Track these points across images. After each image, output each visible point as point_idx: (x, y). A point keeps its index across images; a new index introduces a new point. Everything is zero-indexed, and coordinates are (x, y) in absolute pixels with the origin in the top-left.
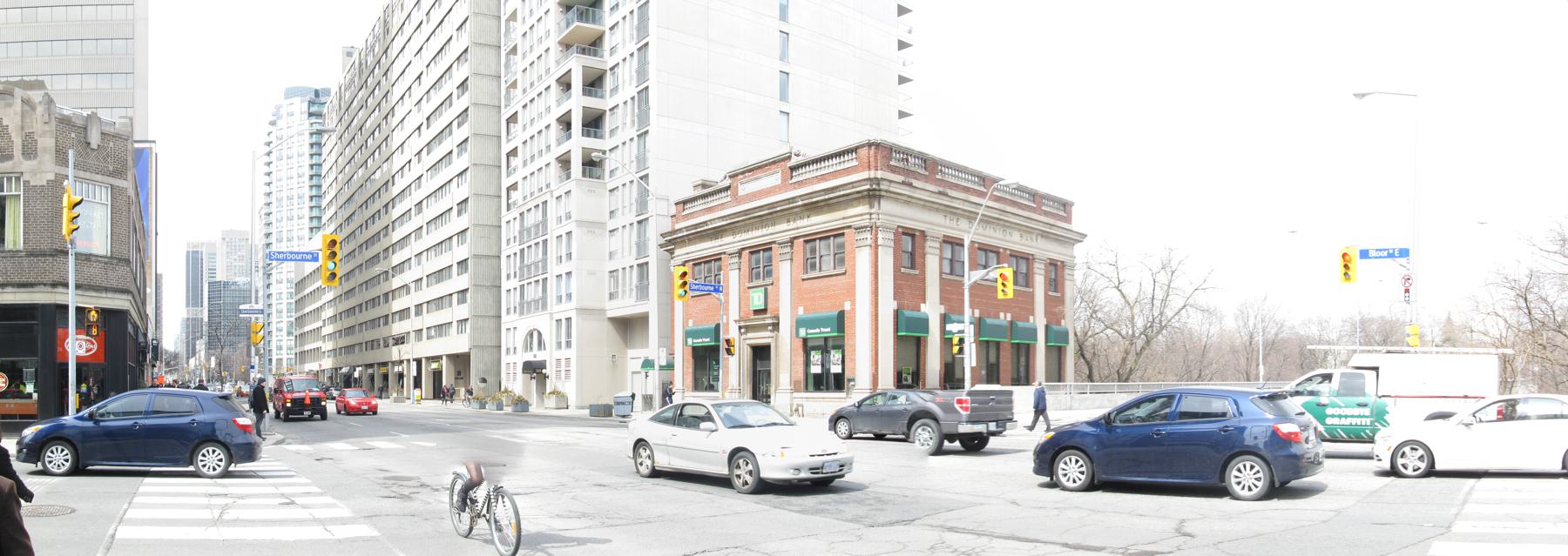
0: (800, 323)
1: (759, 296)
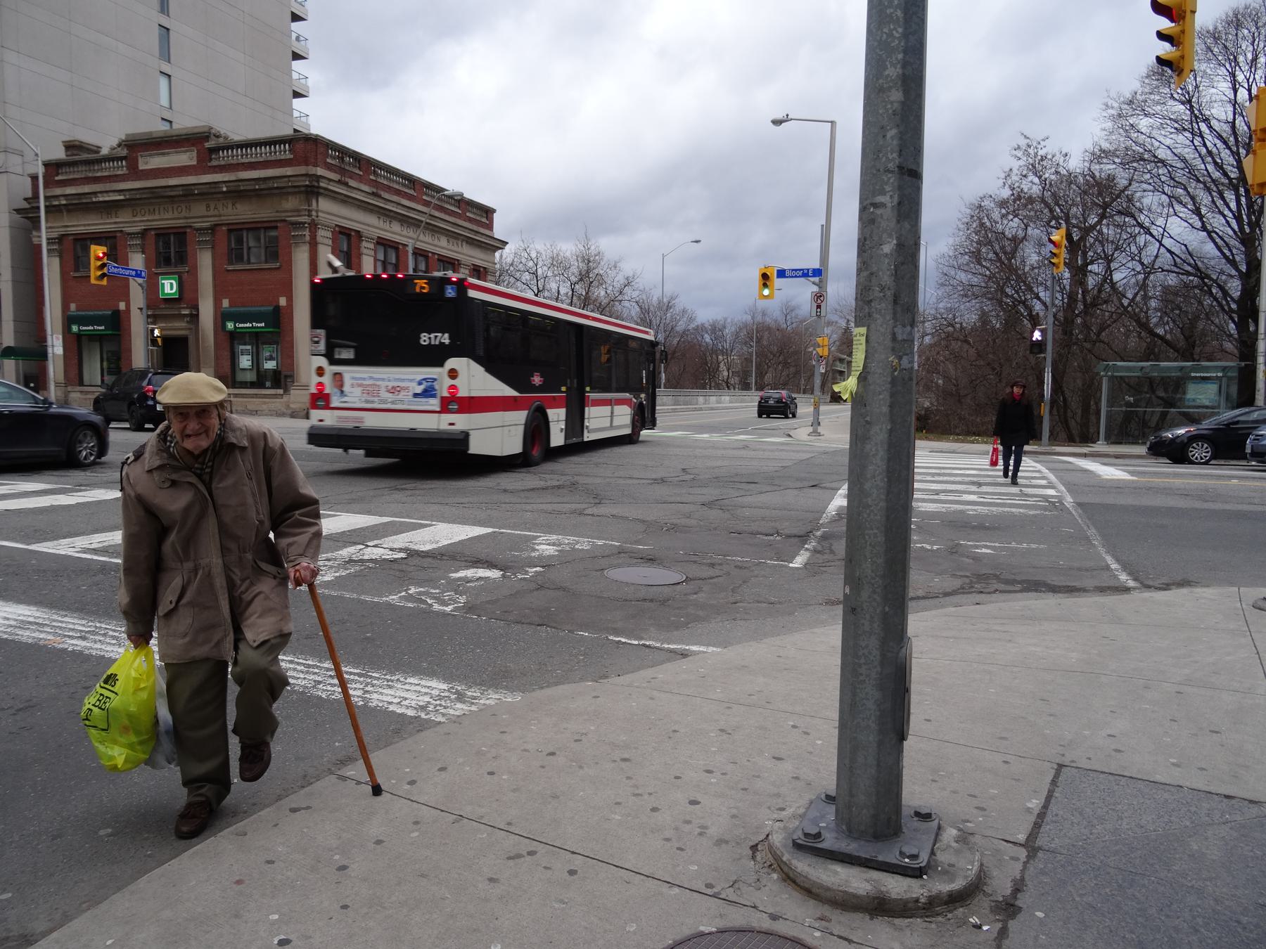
0: (222, 317)
1: (171, 284)
